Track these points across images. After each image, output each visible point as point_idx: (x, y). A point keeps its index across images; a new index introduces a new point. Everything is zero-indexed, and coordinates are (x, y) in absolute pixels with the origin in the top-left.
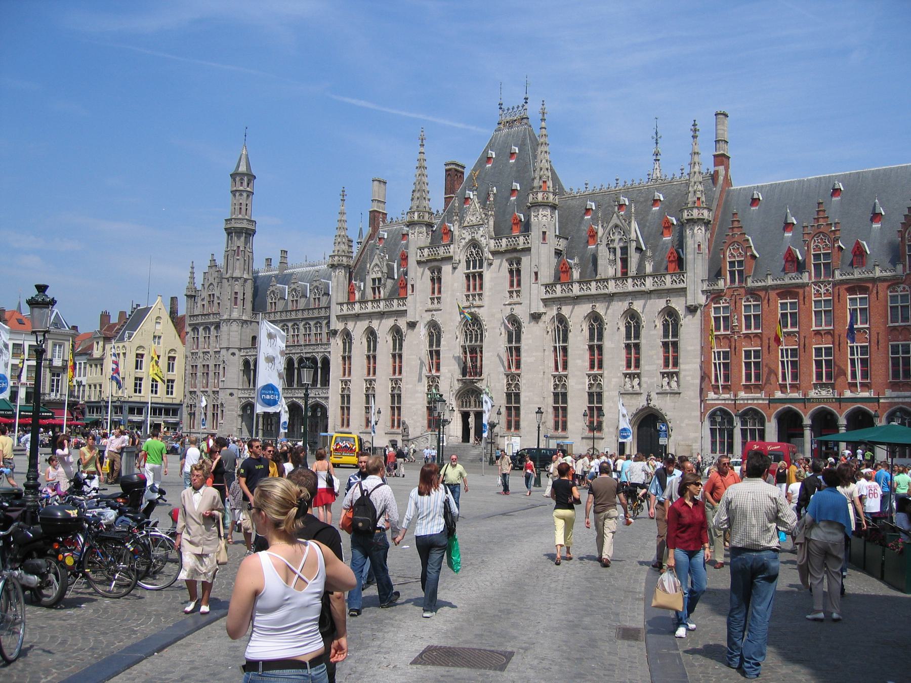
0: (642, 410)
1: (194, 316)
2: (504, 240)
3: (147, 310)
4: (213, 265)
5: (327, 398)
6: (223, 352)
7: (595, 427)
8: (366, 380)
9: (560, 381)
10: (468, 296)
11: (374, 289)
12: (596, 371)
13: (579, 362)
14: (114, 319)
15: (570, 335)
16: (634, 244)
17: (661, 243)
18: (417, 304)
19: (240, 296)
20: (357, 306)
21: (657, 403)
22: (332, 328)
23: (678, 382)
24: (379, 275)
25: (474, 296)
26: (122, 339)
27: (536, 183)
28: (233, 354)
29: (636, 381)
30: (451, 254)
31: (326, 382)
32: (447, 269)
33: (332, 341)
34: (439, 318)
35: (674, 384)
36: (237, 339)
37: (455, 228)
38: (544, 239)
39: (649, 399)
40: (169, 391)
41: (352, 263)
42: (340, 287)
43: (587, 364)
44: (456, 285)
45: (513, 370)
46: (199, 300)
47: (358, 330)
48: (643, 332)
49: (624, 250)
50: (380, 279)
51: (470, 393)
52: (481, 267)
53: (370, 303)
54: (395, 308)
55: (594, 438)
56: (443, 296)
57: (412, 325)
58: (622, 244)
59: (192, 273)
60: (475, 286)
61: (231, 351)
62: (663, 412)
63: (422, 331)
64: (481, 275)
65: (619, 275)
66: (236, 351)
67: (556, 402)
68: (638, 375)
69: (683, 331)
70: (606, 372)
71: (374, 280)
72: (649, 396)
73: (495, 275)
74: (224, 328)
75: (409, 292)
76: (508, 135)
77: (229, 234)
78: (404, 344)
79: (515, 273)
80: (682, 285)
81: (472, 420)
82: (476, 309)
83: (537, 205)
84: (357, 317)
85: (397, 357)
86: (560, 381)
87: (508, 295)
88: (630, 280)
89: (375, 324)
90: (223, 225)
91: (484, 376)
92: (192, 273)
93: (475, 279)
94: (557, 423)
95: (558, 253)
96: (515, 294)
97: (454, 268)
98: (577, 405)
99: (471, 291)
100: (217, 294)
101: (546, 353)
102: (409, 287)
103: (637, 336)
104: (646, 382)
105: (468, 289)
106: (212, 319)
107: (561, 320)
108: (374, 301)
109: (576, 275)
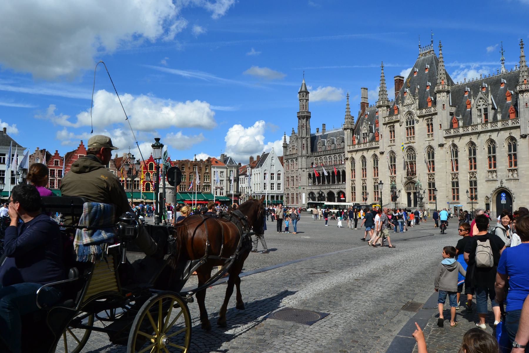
0: (498, 189)
2: (424, 110)
3: (268, 154)
4: (293, 132)
5: (345, 188)
6: (300, 170)
7: (473, 198)
9: (455, 176)
10: (408, 138)
11: (364, 138)
12: (473, 170)
13: (464, 166)
14: (255, 159)
15: (459, 153)
16: (491, 106)
17: (505, 104)
18: (384, 143)
19: (305, 146)
20: (356, 146)
21: (506, 185)
22: (346, 157)
23: (517, 174)
24: (366, 131)
25: (410, 137)
26: (258, 167)
27: (438, 81)
28: (304, 171)
29: (495, 174)
31: (344, 180)
32: (397, 125)
33: (346, 163)
34: (394, 149)
35: (515, 175)
37: (400, 106)
38: (444, 108)
39: (501, 182)
40: (279, 188)
41: (353, 127)
42: (349, 138)
43: (469, 167)
45: (431, 172)
46: (288, 148)
47: (357, 157)
48: (497, 150)
49: (486, 110)
50: (366, 133)
51: (410, 182)
52: (413, 124)
54: (374, 146)
55: (472, 203)
56: (396, 139)
57: (382, 153)
58: (484, 107)
60: (411, 133)
61: (303, 170)
62: (510, 189)
63: (387, 155)
64: (413, 128)
65: (484, 122)
66: (305, 170)
67: (453, 186)
68: (496, 171)
69: (519, 148)
70: (478, 170)
71: (364, 134)
72: (501, 181)
73: (420, 126)
74: (299, 159)
75: (380, 138)
76: (424, 59)
77: (299, 119)
78: (379, 162)
79: (430, 125)
80: (518, 125)
81: (412, 196)
83: (439, 92)
84: (357, 151)
85: (376, 168)
86: (455, 176)
87: (427, 136)
88: (489, 124)
89: (365, 153)
90: (296, 115)
93: (411, 130)
94: (454, 197)
95: (451, 114)
96: (430, 136)
97: (401, 126)
98: (464, 186)
99: (410, 136)
100: (296, 145)
101: (447, 163)
102: (380, 136)
103: (494, 152)
104: (500, 175)
105: (408, 135)
106: (294, 156)
107: (454, 146)
108: (364, 143)
109: (461, 123)
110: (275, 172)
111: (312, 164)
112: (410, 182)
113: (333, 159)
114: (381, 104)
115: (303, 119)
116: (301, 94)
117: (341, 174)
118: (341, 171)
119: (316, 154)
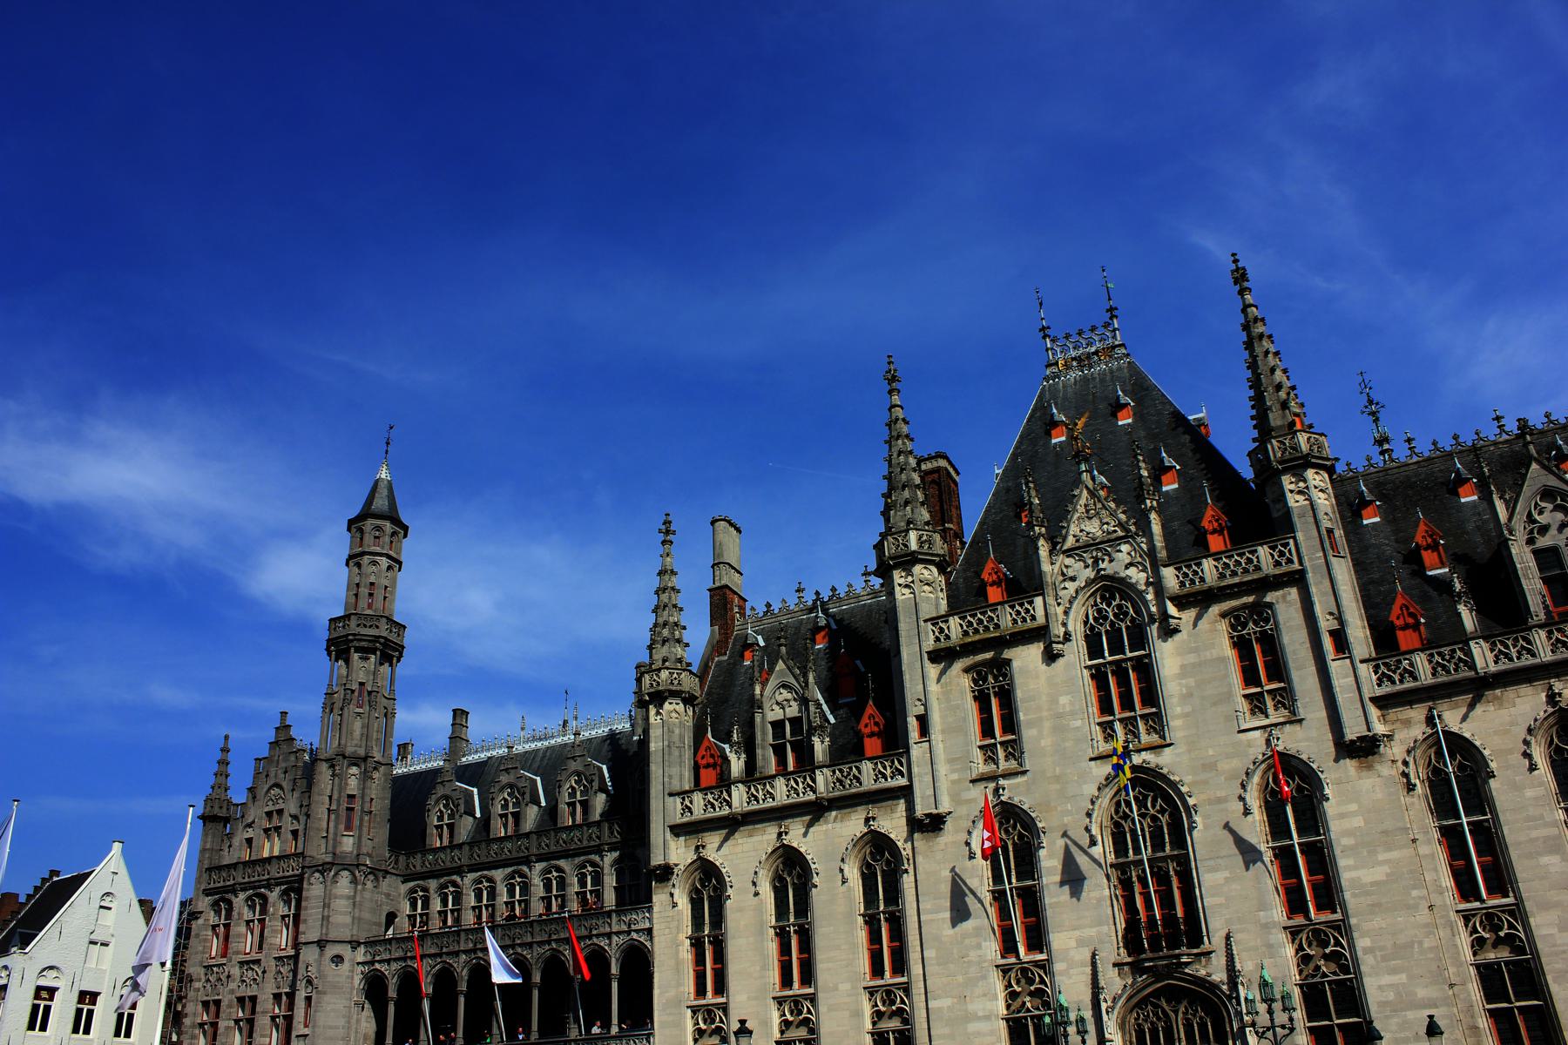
1: (220, 868)
8: (780, 1001)
25: (1129, 724)
28: (338, 959)
30: (1041, 620)
33: (659, 898)
36: (348, 919)
44: (1064, 700)
52: (1139, 640)
53: (780, 783)
56: (1028, 734)
57: (934, 824)
59: (224, 763)
61: (332, 950)
66: (345, 950)
71: (778, 726)
74: (314, 889)
76: (1085, 380)
82: (1145, 756)
87: (1244, 706)
91: (1216, 941)
92: (224, 763)
101: (1424, 850)
110: (103, 987)
111: (391, 918)
112: (1156, 994)
113: (538, 889)
114: (914, 546)
115: (365, 652)
116: (370, 523)
117: (614, 970)
118: (613, 949)
119: (417, 863)
